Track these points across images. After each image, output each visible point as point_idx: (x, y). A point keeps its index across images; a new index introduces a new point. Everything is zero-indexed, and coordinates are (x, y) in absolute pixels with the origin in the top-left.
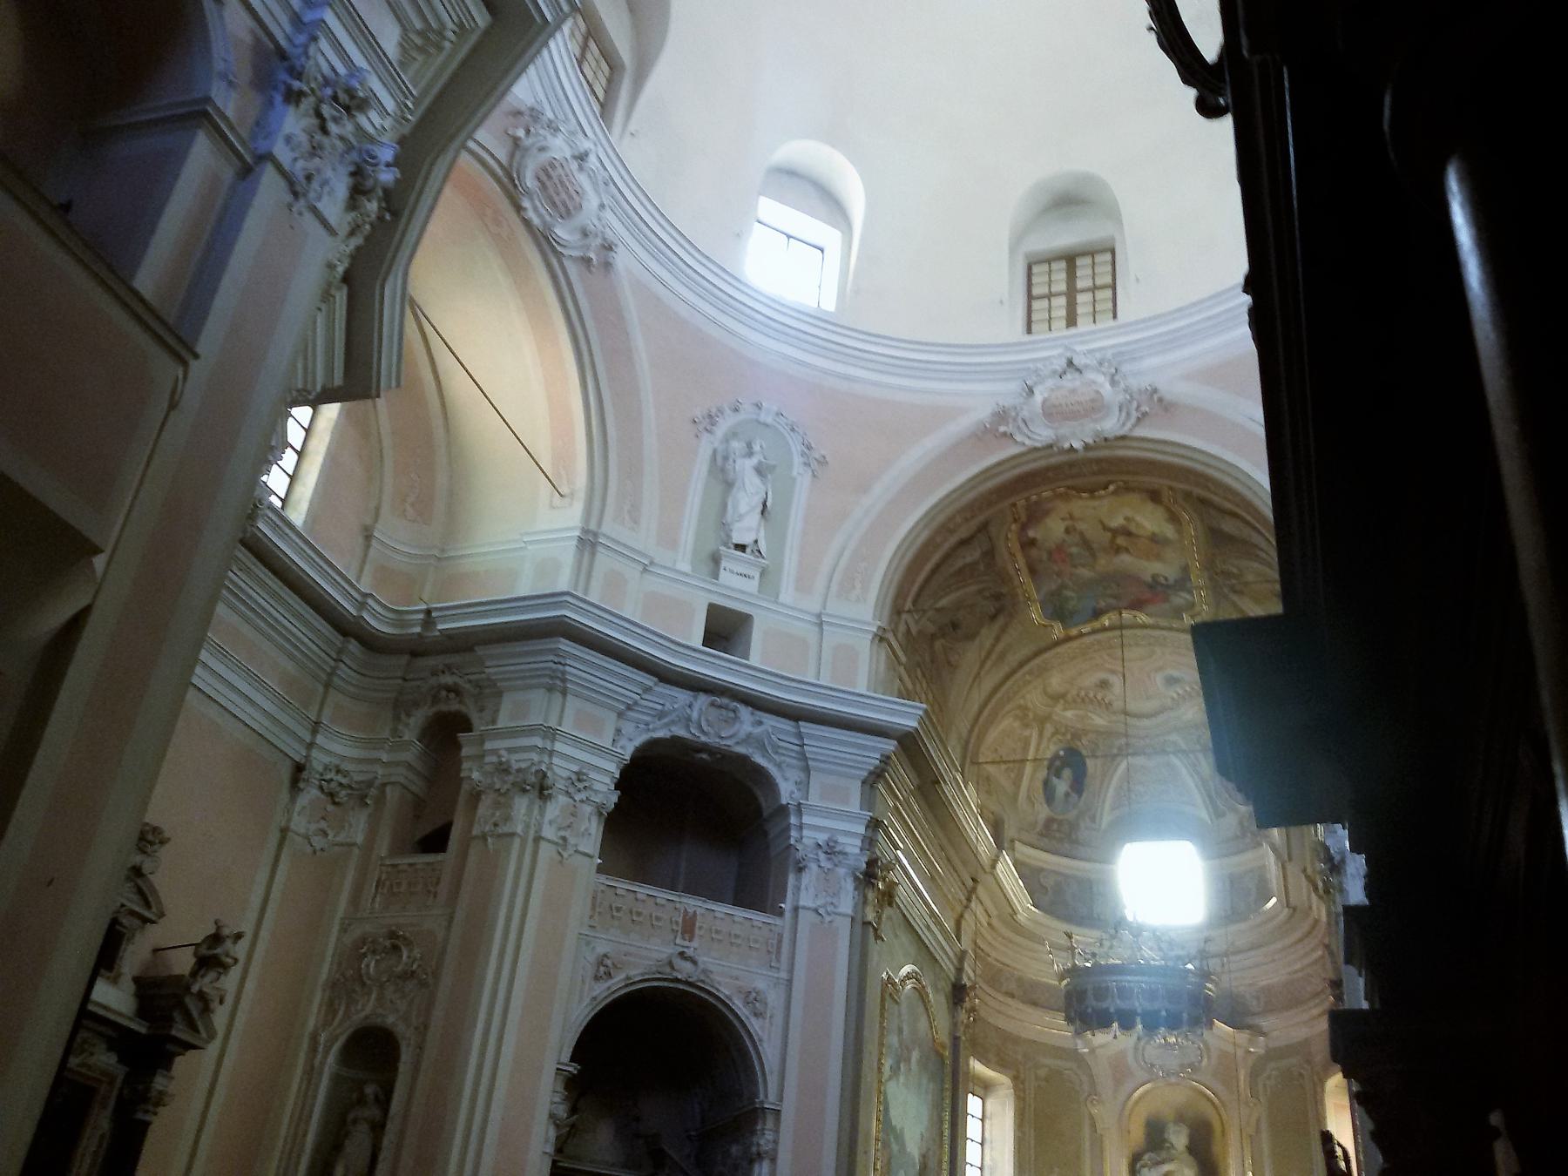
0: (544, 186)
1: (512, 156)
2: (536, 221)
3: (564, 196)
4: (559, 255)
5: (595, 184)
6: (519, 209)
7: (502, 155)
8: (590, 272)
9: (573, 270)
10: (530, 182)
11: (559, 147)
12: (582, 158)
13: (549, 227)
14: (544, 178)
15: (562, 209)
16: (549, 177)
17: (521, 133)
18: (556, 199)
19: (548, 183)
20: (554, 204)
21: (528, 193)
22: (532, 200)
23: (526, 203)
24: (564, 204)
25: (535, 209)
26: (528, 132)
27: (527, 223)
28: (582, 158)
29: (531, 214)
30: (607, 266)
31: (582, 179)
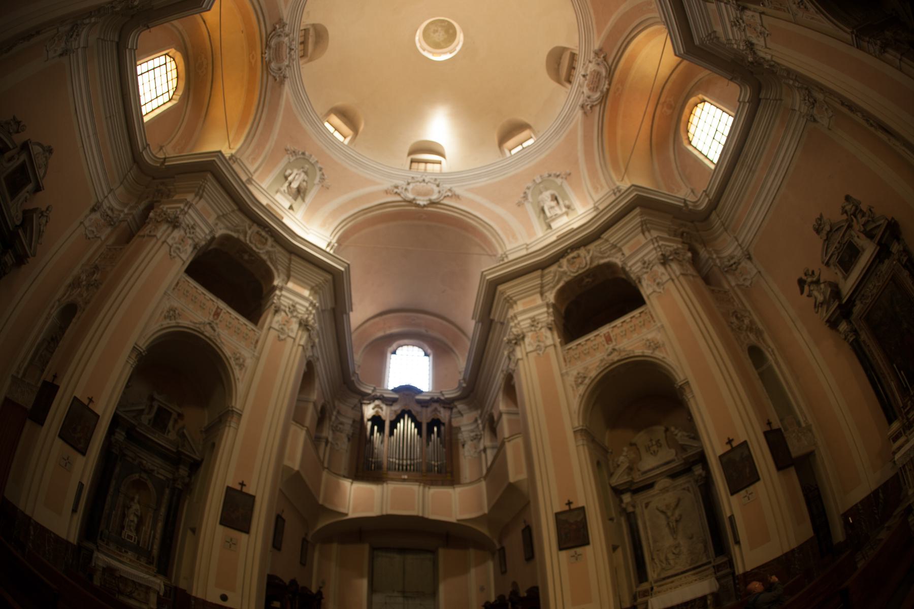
0: (597, 87)
1: (596, 105)
2: (607, 82)
3: (595, 79)
4: (610, 68)
5: (587, 67)
6: (608, 90)
7: (597, 108)
8: (606, 55)
9: (610, 61)
10: (598, 95)
11: (585, 90)
12: (584, 76)
13: (606, 78)
14: (595, 90)
15: (598, 77)
16: (594, 88)
17: (588, 107)
18: (597, 80)
19: (595, 86)
20: (599, 80)
21: (602, 92)
22: (603, 89)
23: (605, 90)
24: (596, 78)
25: (604, 85)
26: (588, 105)
27: (610, 84)
28: (584, 76)
29: (606, 86)
30: (601, 50)
31: (588, 72)
